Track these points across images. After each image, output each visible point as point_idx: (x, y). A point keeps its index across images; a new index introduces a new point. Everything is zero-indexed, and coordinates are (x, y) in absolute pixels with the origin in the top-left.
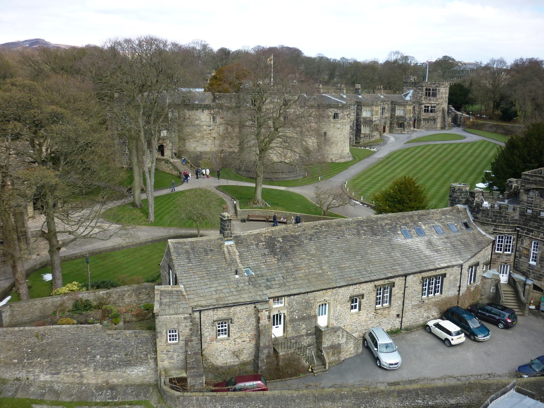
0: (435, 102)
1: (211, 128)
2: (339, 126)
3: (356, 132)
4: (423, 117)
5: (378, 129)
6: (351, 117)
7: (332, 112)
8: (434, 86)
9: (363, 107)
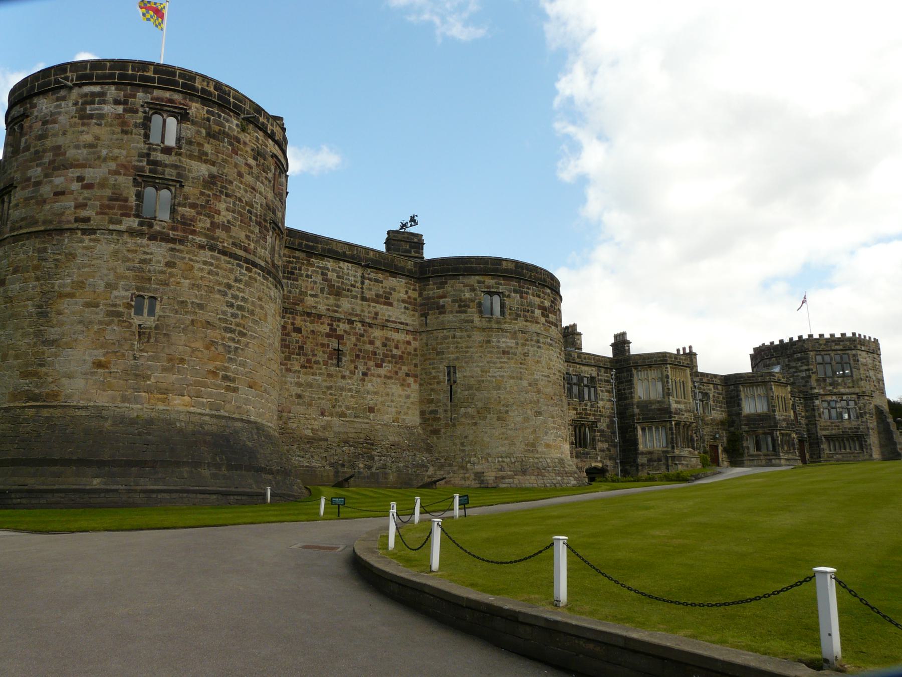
0: (852, 390)
2: (506, 342)
3: (623, 451)
4: (825, 433)
5: (692, 440)
6: (601, 404)
7: (473, 290)
8: (837, 347)
9: (634, 372)
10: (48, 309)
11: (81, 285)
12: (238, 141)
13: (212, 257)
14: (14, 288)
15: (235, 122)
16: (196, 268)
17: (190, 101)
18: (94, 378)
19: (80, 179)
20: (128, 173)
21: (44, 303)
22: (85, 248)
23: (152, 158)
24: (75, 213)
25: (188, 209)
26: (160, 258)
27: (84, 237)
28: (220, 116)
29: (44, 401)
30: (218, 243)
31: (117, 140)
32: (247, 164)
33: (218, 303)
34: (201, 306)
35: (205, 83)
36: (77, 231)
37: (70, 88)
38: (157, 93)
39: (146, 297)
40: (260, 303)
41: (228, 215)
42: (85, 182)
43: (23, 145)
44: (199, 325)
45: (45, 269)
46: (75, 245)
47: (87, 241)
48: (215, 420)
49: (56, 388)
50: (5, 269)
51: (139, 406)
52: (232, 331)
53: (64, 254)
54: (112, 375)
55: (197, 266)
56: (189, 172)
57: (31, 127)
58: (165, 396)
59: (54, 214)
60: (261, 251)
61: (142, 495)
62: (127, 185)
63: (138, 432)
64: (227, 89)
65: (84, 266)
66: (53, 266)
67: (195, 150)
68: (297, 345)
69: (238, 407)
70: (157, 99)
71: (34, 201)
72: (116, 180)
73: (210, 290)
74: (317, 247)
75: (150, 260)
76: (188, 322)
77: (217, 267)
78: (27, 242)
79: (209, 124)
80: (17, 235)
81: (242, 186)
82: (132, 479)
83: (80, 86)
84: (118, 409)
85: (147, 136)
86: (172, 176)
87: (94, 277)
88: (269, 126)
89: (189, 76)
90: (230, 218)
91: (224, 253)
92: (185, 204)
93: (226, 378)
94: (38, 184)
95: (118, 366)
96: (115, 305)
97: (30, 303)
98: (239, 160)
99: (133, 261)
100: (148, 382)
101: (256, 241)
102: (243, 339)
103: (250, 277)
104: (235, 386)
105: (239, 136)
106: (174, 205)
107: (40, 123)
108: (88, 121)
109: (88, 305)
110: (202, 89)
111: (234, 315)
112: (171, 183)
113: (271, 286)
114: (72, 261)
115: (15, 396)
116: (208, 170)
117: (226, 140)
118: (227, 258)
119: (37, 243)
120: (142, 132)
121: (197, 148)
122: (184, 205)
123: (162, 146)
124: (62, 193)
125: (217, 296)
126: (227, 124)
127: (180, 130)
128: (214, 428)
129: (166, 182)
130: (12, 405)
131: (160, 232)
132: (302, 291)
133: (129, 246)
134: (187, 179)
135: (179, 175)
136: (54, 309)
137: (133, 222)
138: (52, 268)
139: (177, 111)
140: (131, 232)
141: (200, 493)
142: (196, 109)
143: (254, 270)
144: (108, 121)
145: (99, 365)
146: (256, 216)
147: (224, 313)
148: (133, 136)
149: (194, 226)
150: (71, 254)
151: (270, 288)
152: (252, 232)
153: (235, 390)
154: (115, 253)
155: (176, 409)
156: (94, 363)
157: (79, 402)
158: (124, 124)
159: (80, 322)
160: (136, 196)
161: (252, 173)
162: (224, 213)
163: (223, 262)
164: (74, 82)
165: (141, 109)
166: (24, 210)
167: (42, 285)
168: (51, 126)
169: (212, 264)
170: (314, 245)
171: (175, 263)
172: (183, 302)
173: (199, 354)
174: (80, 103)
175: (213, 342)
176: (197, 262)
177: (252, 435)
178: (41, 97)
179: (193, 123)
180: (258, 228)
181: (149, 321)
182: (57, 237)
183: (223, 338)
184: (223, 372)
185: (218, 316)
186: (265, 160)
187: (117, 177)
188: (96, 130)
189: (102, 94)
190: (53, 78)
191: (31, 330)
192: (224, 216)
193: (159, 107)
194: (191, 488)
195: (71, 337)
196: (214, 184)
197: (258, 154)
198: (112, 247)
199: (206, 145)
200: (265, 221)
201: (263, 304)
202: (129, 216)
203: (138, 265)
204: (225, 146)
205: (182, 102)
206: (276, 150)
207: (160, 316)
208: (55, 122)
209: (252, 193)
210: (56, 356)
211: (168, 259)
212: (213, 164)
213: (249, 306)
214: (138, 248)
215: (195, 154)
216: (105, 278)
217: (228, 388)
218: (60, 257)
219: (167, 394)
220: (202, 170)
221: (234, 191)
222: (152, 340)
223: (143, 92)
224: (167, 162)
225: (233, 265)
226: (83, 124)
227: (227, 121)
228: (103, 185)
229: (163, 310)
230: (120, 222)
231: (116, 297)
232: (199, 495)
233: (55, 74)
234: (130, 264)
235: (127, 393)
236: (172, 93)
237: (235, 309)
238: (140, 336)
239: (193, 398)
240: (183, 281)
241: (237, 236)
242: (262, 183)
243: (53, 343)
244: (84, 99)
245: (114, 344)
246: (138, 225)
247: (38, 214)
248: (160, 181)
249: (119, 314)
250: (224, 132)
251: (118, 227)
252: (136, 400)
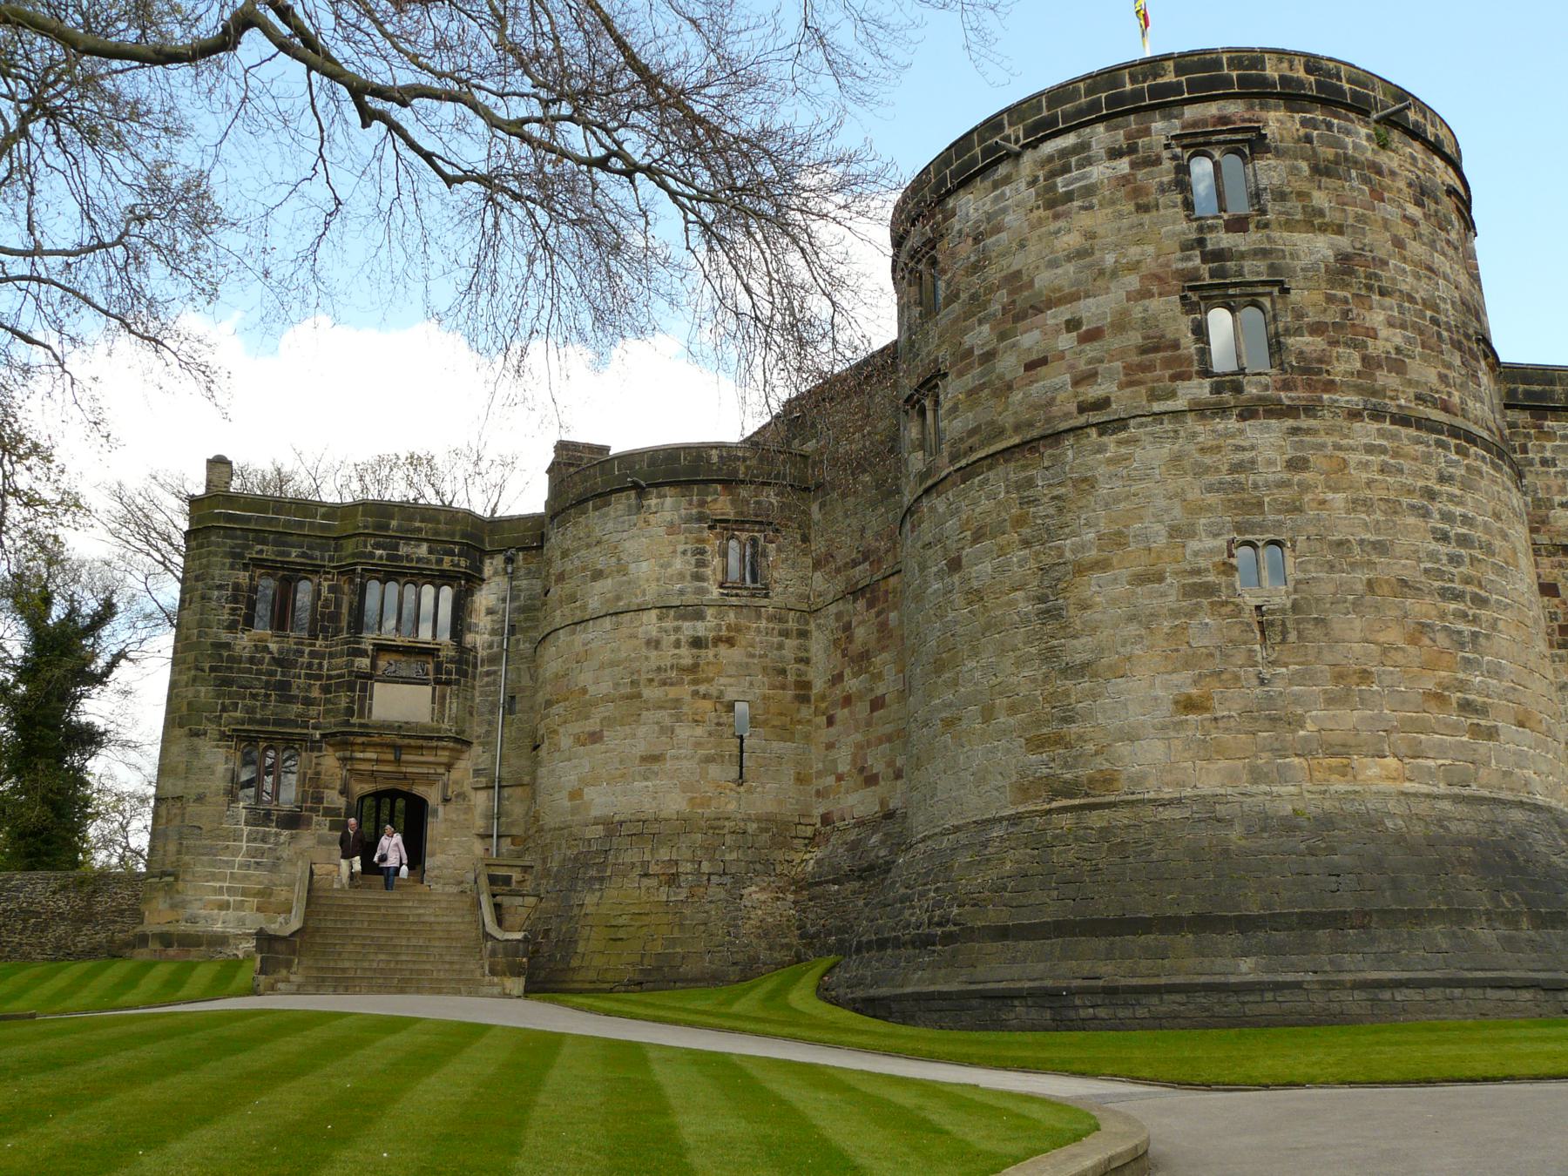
1: (701, 629)
10: (1061, 601)
11: (1118, 539)
12: (1379, 172)
13: (1381, 434)
14: (981, 570)
15: (1364, 131)
16: (1352, 464)
17: (1261, 109)
18: (1182, 735)
19: (1072, 325)
20: (1168, 288)
21: (1048, 591)
22: (1110, 461)
23: (1210, 247)
24: (1076, 395)
25: (1307, 338)
26: (1273, 454)
27: (1105, 439)
28: (1329, 126)
29: (1087, 795)
30: (1387, 401)
31: (1131, 227)
32: (1406, 218)
33: (1414, 535)
34: (1381, 548)
35: (1285, 65)
36: (1088, 430)
37: (1018, 155)
38: (1190, 112)
39: (1260, 544)
40: (1499, 525)
41: (1395, 335)
42: (1084, 328)
43: (941, 294)
44: (1386, 589)
45: (1039, 521)
46: (1090, 459)
47: (1112, 447)
48: (1464, 809)
49: (1106, 765)
50: (956, 538)
51: (1292, 789)
52: (1458, 596)
53: (1069, 483)
54: (1221, 724)
55: (1354, 458)
56: (1293, 259)
57: (953, 255)
58: (1345, 761)
59: (1036, 407)
60: (1475, 407)
61: (1358, 995)
62: (1170, 314)
63: (1308, 847)
64: (1331, 65)
65: (1117, 501)
66: (1052, 511)
67: (1295, 207)
68: (1555, 624)
69: (1505, 774)
70: (1195, 124)
71: (986, 391)
72: (1146, 310)
73: (1393, 508)
74: (1553, 392)
75: (1253, 462)
76: (1360, 587)
77: (1396, 455)
78: (991, 474)
79: (1313, 149)
80: (968, 465)
81: (1408, 268)
82: (1323, 957)
83: (1034, 145)
84: (1249, 800)
85: (1188, 205)
86: (1258, 274)
87: (1141, 518)
88: (1429, 128)
89: (1249, 59)
90: (1398, 341)
91: (1403, 420)
92: (1300, 328)
93: (1466, 706)
94: (989, 356)
95: (1230, 704)
96: (1197, 572)
97: (1020, 594)
98: (1389, 210)
99: (1217, 470)
100: (1302, 733)
101: (1461, 386)
102: (1484, 613)
103: (1468, 468)
104: (1489, 724)
105: (1378, 159)
106: (1277, 334)
107: (970, 241)
108: (1065, 207)
109: (1141, 579)
110: (1281, 77)
111: (1455, 560)
112: (1260, 290)
113: (1509, 483)
114: (1090, 493)
115: (1024, 791)
116: (1332, 246)
117: (1354, 173)
118: (1412, 432)
119: (1010, 472)
120: (1179, 198)
121: (1299, 205)
122: (1298, 332)
123: (1226, 216)
124: (1043, 361)
125: (1411, 520)
126: (1349, 140)
127: (1255, 175)
128: (1470, 826)
129: (1249, 290)
130: (1021, 809)
131: (1260, 398)
132: (1539, 499)
133: (1200, 439)
134: (1292, 273)
135: (1272, 267)
136: (1072, 601)
137: (1201, 389)
138: (1052, 517)
139: (1239, 137)
140: (1201, 410)
141: (1492, 987)
142: (1277, 122)
143: (1473, 450)
144: (1104, 197)
145: (1189, 705)
146: (1449, 330)
147: (1433, 556)
148: (1162, 212)
149: (1328, 372)
150: (1085, 480)
151: (1509, 490)
152: (1449, 366)
153: (1492, 733)
154: (1176, 459)
155: (1374, 788)
156: (1176, 703)
157: (1159, 790)
158: (1137, 192)
159: (1131, 618)
160: (1194, 332)
161: (1420, 235)
162: (1384, 332)
163: (1406, 441)
164: (1022, 142)
165: (1166, 154)
166: (970, 415)
167: (1037, 554)
168: (993, 239)
169: (1384, 450)
170: (1544, 391)
171: (1305, 460)
172: (1340, 543)
173: (1399, 657)
174: (1041, 179)
175: (1423, 625)
176: (1353, 449)
177: (1555, 839)
178: (961, 192)
179: (1279, 153)
180: (1457, 354)
181: (1278, 596)
182: (1050, 451)
183: (1443, 615)
184: (1459, 694)
185: (1422, 566)
186: (1437, 203)
187: (1147, 302)
188: (1085, 220)
189: (1083, 147)
190: (978, 150)
191: (1033, 650)
192: (1387, 340)
193: (1201, 140)
194: (1469, 975)
195: (1117, 653)
196: (1351, 272)
197: (1422, 193)
198: (1167, 449)
199: (1316, 194)
200: (1468, 337)
201: (1505, 527)
202: (1190, 378)
203: (1228, 478)
204: (1355, 186)
205: (1247, 116)
206: (1451, 178)
207: (1298, 582)
208: (998, 229)
209: (1430, 278)
210: (1095, 696)
211: (1290, 453)
212: (1340, 230)
213: (1478, 534)
214: (1221, 442)
215: (1297, 217)
216: (1166, 517)
217: (1476, 731)
218: (1063, 490)
219: (1347, 755)
220: (1319, 247)
221: (1394, 280)
222: (1292, 637)
223: (1163, 118)
224: (1243, 248)
225: (1429, 446)
226: (1056, 217)
227: (1348, 133)
228: (1120, 326)
229: (1300, 566)
230: (1173, 394)
231: (1196, 554)
232: (1490, 993)
233: (982, 140)
234: (1211, 478)
235: (1260, 762)
236: (1222, 103)
237: (1454, 544)
238: (1262, 632)
239: (1407, 760)
240: (1330, 496)
241: (1423, 379)
242: (1444, 254)
243: (1082, 670)
244: (1047, 168)
245: (1212, 655)
246: (1211, 393)
247: (1000, 414)
248: (1237, 291)
249: (1209, 590)
250: (1347, 158)
251: (1169, 405)
252: (1283, 776)
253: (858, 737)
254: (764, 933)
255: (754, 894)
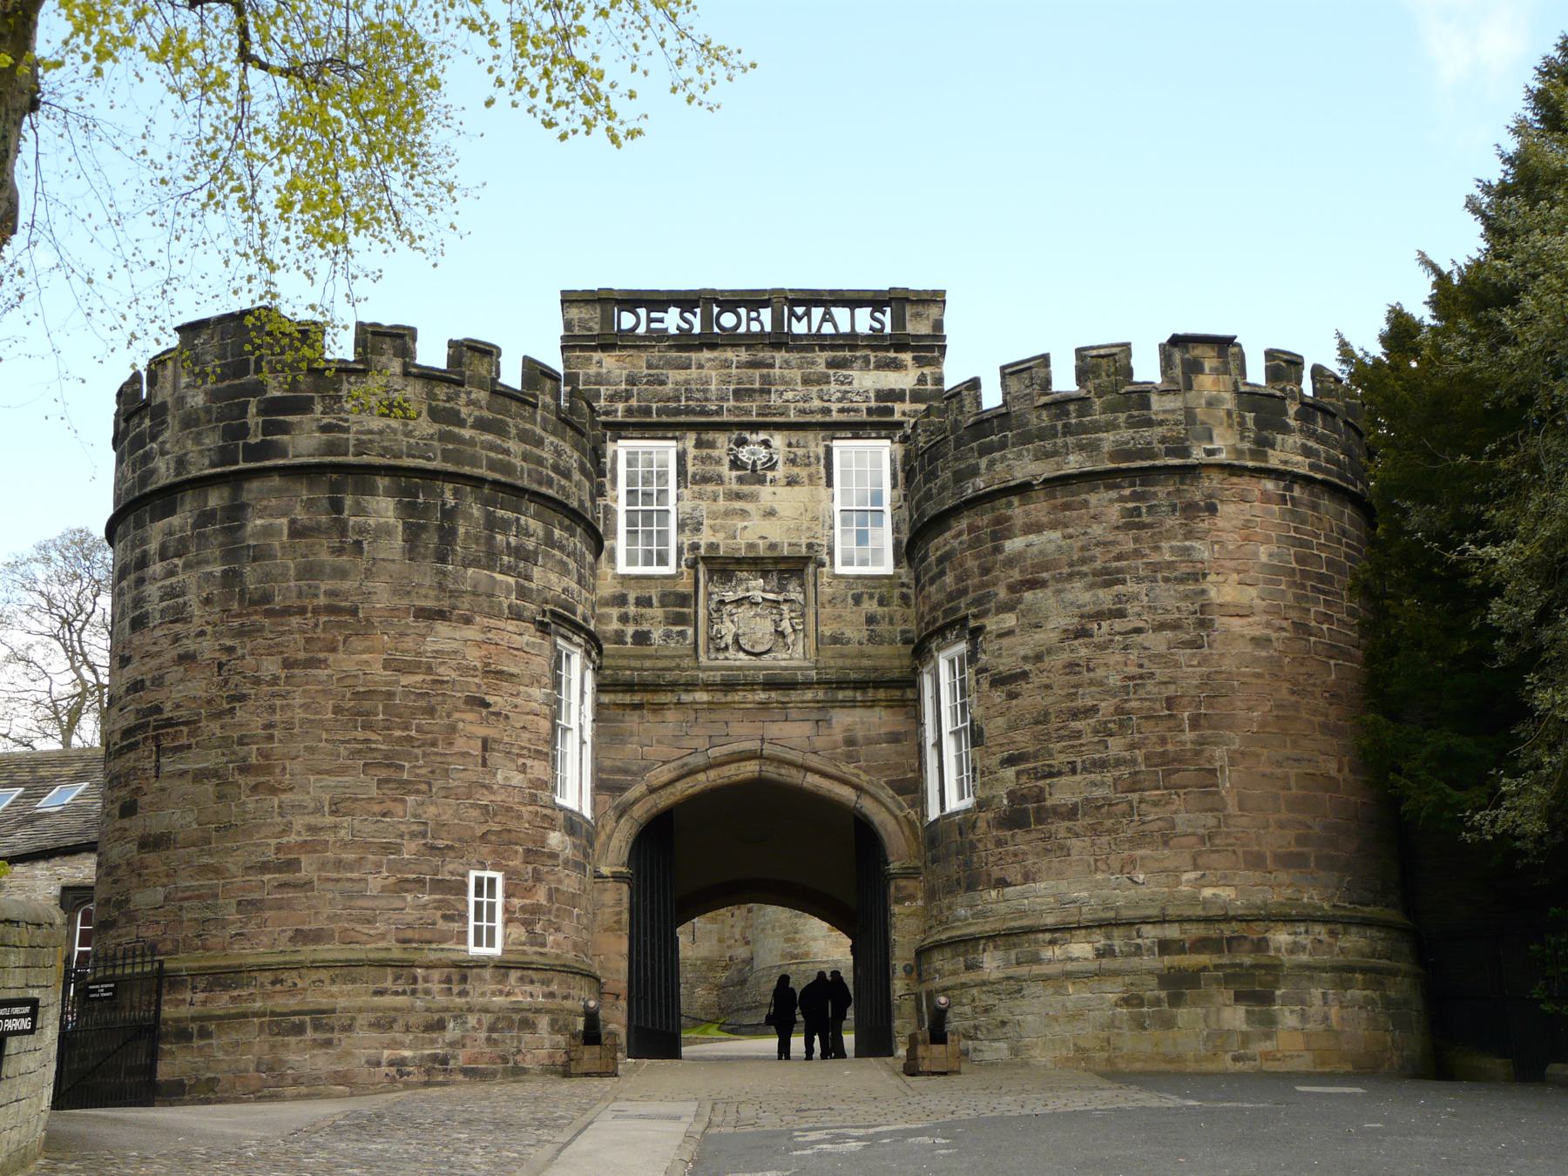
115: (783, 956)
253: (743, 924)
254: (703, 1008)
255: (699, 991)
